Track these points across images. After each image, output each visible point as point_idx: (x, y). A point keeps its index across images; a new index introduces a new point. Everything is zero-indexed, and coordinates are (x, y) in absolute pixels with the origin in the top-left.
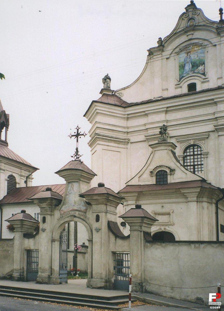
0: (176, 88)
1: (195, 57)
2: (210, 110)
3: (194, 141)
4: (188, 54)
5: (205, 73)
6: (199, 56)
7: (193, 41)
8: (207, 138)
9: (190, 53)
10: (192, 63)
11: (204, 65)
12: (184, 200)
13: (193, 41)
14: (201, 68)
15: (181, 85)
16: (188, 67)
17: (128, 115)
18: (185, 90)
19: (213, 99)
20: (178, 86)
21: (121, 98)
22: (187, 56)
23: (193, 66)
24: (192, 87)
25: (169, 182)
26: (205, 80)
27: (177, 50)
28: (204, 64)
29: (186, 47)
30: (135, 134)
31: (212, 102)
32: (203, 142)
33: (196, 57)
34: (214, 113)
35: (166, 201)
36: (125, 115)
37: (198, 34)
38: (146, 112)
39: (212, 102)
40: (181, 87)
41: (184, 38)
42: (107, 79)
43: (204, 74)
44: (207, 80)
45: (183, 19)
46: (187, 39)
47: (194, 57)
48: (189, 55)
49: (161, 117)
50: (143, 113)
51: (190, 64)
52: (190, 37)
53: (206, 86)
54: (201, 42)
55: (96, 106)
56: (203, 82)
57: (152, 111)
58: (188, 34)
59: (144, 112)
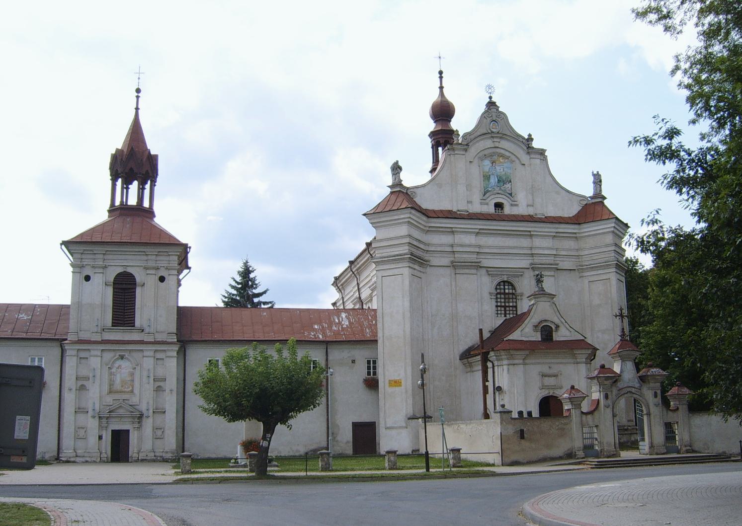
0: (481, 204)
1: (501, 169)
2: (525, 242)
3: (508, 276)
4: (492, 163)
5: (512, 193)
6: (505, 170)
7: (498, 150)
8: (522, 275)
11: (510, 183)
12: (572, 361)
13: (498, 150)
14: (508, 186)
15: (487, 201)
16: (493, 180)
17: (430, 227)
18: (491, 209)
19: (530, 231)
20: (483, 202)
21: (414, 199)
22: (492, 165)
24: (499, 206)
25: (554, 339)
26: (513, 203)
27: (481, 154)
28: (510, 182)
29: (491, 155)
30: (438, 255)
31: (529, 234)
32: (517, 279)
33: (502, 170)
34: (531, 248)
35: (553, 361)
36: (425, 226)
37: (504, 144)
38: (454, 230)
39: (529, 234)
40: (487, 204)
41: (488, 143)
42: (396, 169)
43: (511, 194)
44: (515, 203)
45: (484, 117)
47: (499, 170)
48: (494, 165)
50: (449, 230)
51: (496, 177)
52: (497, 144)
53: (516, 211)
54: (507, 154)
55: (410, 213)
56: (512, 205)
57: (461, 230)
58: (495, 140)
59: (452, 228)
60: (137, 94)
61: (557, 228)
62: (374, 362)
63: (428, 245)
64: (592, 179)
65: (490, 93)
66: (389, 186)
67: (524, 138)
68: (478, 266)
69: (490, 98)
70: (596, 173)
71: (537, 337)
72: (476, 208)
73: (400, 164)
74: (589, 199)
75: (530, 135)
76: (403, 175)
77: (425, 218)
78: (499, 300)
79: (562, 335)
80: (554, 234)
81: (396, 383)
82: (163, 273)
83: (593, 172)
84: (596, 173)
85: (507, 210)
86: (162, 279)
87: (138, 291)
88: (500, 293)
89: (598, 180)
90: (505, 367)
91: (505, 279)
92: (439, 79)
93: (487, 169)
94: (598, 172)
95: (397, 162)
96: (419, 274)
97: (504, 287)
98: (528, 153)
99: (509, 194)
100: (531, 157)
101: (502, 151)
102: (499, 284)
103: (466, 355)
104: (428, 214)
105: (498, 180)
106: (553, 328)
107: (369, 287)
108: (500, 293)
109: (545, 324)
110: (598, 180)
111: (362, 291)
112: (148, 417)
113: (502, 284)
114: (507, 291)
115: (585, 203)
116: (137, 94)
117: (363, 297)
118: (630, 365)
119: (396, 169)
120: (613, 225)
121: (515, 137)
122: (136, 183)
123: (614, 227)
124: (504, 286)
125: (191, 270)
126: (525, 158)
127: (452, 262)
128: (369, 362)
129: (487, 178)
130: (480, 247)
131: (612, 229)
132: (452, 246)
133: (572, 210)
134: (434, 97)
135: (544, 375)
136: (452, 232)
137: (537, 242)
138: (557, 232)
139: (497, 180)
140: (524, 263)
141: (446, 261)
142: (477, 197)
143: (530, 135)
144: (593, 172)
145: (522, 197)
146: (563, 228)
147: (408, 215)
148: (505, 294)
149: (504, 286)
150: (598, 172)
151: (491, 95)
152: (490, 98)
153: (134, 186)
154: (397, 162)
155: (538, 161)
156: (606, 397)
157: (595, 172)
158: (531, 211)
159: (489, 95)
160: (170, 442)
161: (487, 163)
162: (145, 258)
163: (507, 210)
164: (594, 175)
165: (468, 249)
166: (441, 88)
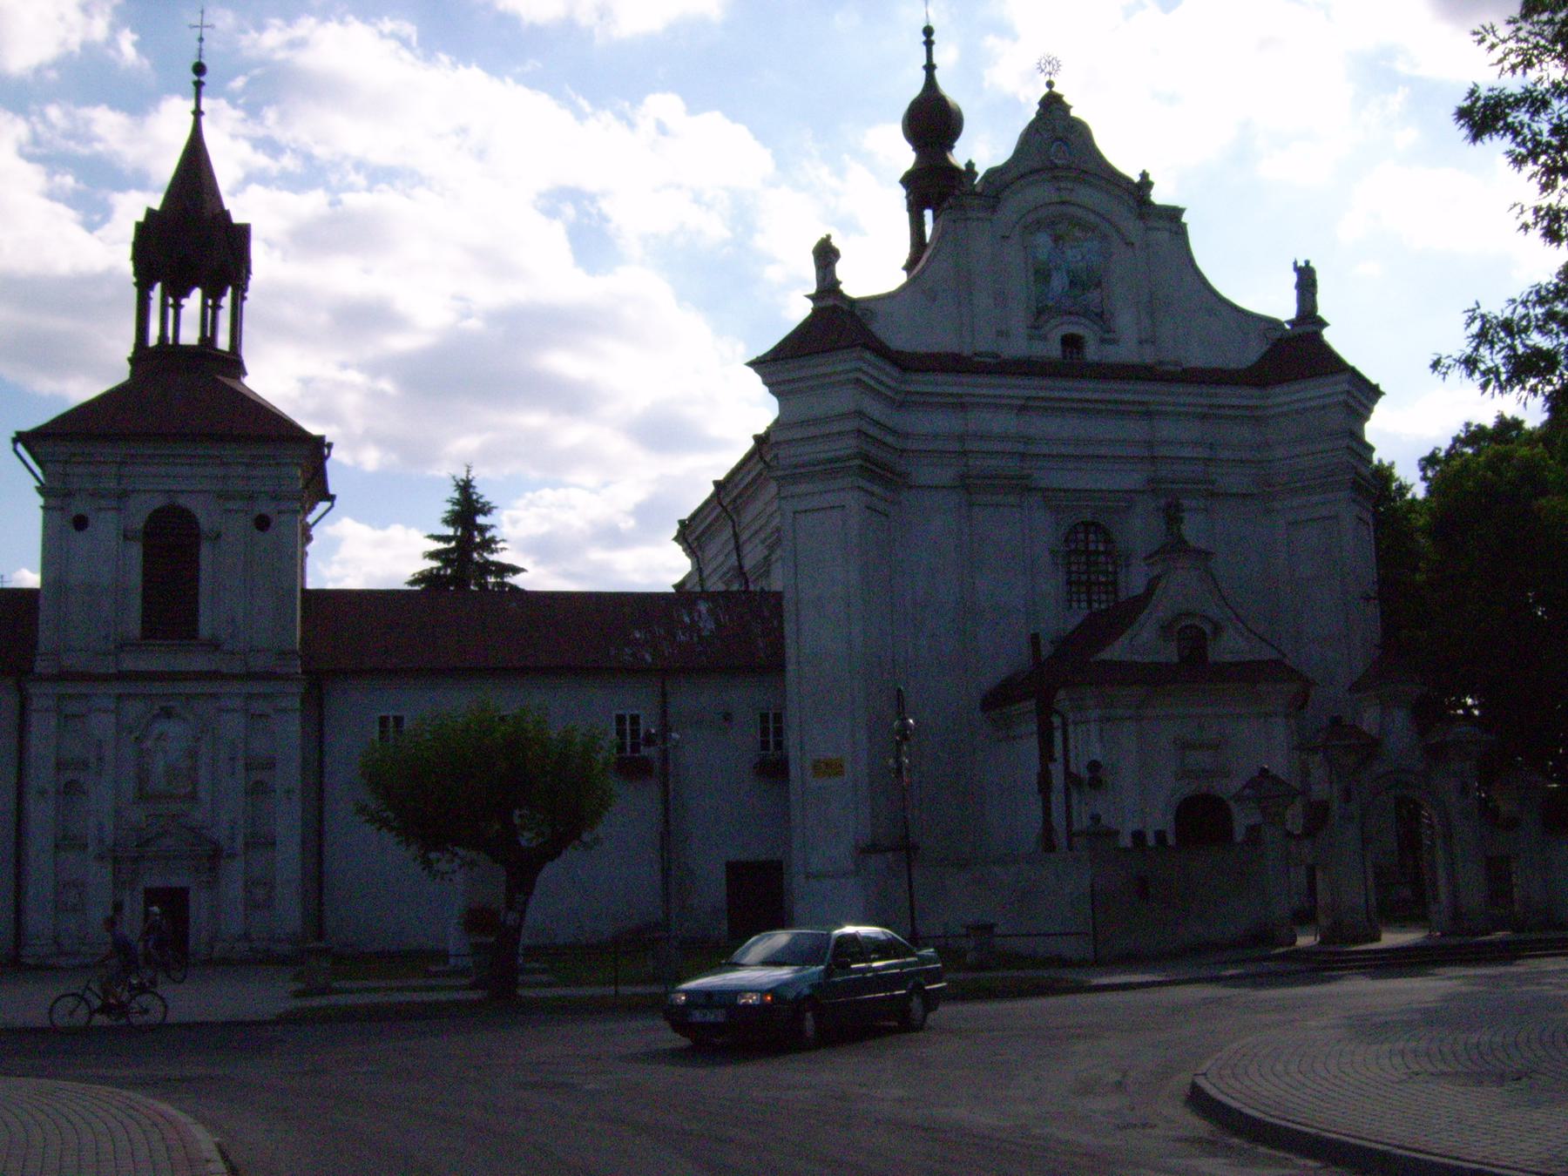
0: (1031, 338)
2: (1134, 429)
5: (1102, 312)
7: (1072, 209)
9: (1061, 242)
10: (1068, 272)
11: (1099, 290)
13: (1072, 209)
14: (1093, 296)
15: (1042, 331)
16: (1058, 283)
18: (1053, 350)
20: (1036, 328)
23: (1072, 284)
26: (1106, 336)
40: (1044, 338)
42: (826, 255)
43: (1100, 315)
46: (1055, 198)
49: (1004, 422)
52: (1065, 196)
55: (861, 359)
56: (1103, 341)
60: (196, 78)
61: (1216, 395)
62: (778, 718)
63: (906, 436)
64: (1294, 278)
65: (1050, 74)
66: (808, 297)
67: (1128, 181)
68: (1023, 487)
69: (1050, 84)
70: (1303, 265)
71: (1170, 653)
72: (1018, 346)
73: (835, 242)
74: (1288, 327)
75: (1144, 175)
76: (841, 270)
77: (895, 373)
78: (1074, 568)
79: (1230, 647)
80: (1206, 410)
81: (829, 768)
82: (265, 507)
83: (1295, 263)
84: (1303, 265)
85: (1092, 352)
86: (263, 523)
87: (205, 553)
88: (1075, 552)
89: (1306, 280)
90: (1094, 728)
91: (1088, 518)
92: (924, 48)
93: (1043, 255)
94: (1307, 263)
95: (829, 237)
96: (882, 506)
97: (1087, 538)
98: (1141, 217)
99: (1097, 315)
100: (1149, 225)
101: (1079, 212)
102: (1074, 530)
103: (997, 699)
104: (905, 363)
105: (1071, 282)
106: (1207, 628)
107: (763, 542)
108: (1075, 552)
109: (1189, 622)
110: (1306, 280)
111: (745, 552)
112: (233, 856)
113: (1081, 529)
114: (1092, 547)
115: (1278, 334)
116: (196, 78)
117: (748, 563)
118: (1400, 720)
119: (826, 255)
120: (1346, 387)
121: (1112, 178)
122: (197, 294)
123: (1348, 392)
124: (1087, 534)
125: (336, 502)
126: (1132, 227)
127: (962, 477)
128: (764, 718)
129: (1042, 275)
130: (1028, 440)
131: (1341, 398)
132: (962, 438)
133: (1252, 352)
134: (914, 87)
135: (1185, 746)
136: (961, 405)
137: (1167, 430)
138: (1210, 406)
139: (1067, 283)
140: (1133, 479)
141: (946, 475)
142: (1018, 321)
143: (1144, 175)
144: (1295, 263)
145: (1126, 322)
146: (1229, 396)
147: (853, 365)
148: (1088, 553)
149: (1087, 534)
150: (1307, 263)
151: (1052, 78)
152: (1050, 84)
153: (193, 303)
154: (829, 237)
155: (1166, 235)
156: (1347, 796)
157: (1301, 263)
158: (1148, 356)
159: (1047, 78)
160: (289, 914)
161: (1043, 240)
162: (219, 471)
163: (1092, 352)
164: (1297, 269)
165: (1000, 447)
166: (930, 68)
